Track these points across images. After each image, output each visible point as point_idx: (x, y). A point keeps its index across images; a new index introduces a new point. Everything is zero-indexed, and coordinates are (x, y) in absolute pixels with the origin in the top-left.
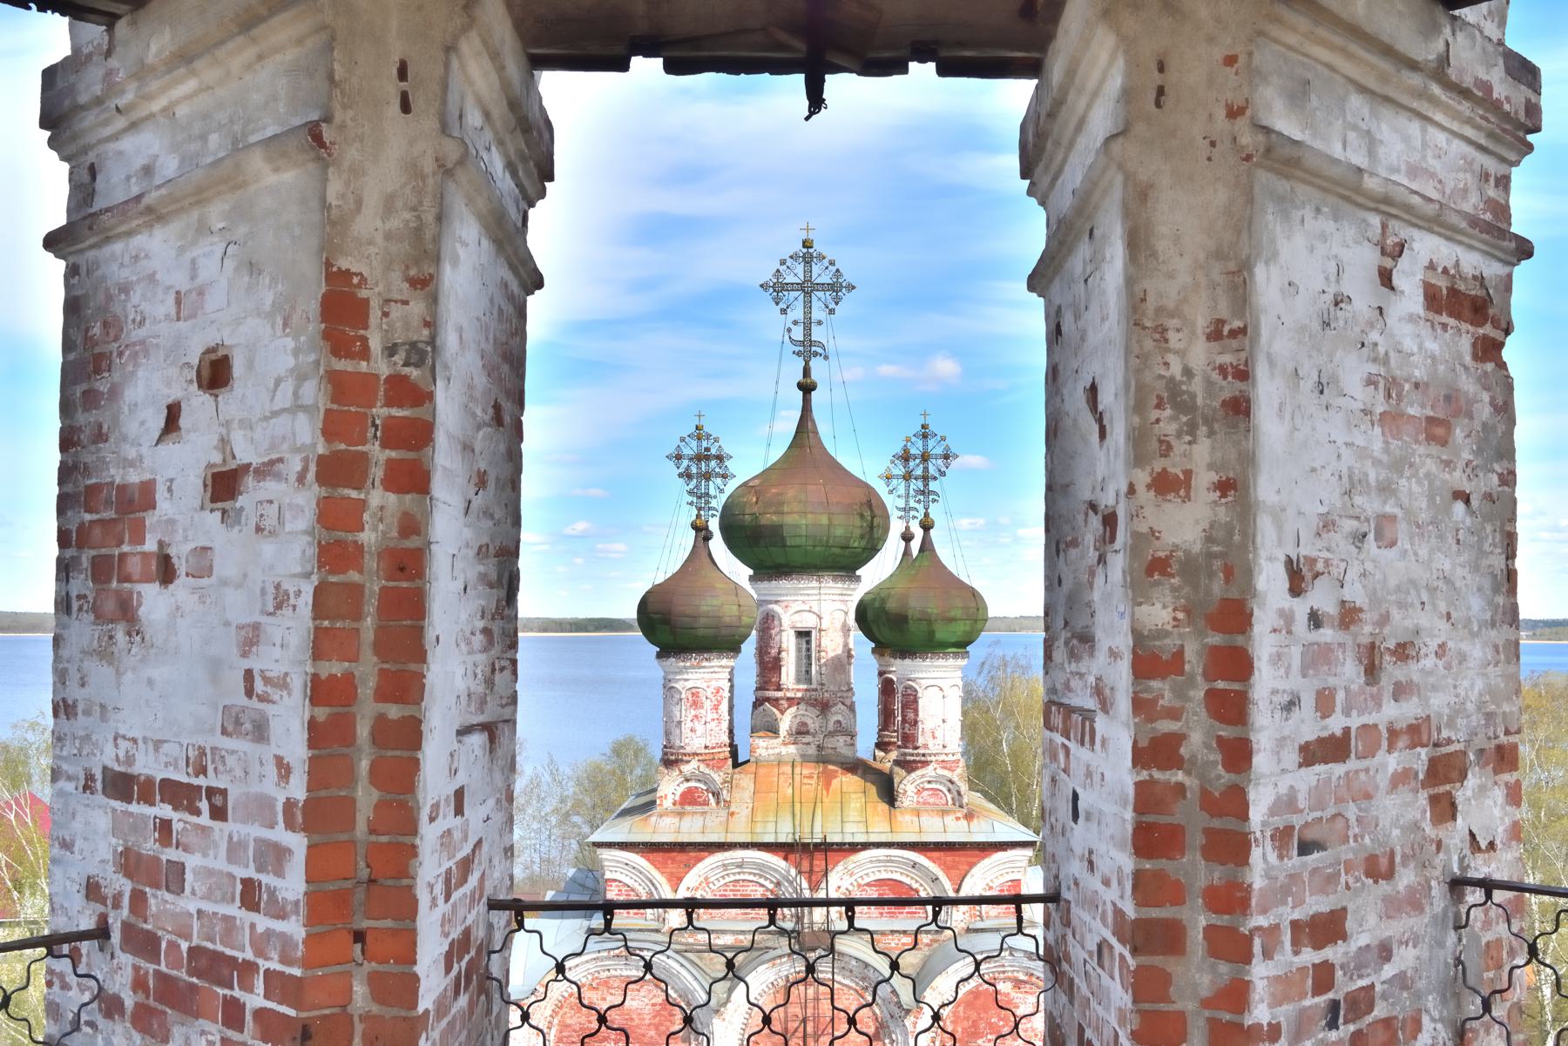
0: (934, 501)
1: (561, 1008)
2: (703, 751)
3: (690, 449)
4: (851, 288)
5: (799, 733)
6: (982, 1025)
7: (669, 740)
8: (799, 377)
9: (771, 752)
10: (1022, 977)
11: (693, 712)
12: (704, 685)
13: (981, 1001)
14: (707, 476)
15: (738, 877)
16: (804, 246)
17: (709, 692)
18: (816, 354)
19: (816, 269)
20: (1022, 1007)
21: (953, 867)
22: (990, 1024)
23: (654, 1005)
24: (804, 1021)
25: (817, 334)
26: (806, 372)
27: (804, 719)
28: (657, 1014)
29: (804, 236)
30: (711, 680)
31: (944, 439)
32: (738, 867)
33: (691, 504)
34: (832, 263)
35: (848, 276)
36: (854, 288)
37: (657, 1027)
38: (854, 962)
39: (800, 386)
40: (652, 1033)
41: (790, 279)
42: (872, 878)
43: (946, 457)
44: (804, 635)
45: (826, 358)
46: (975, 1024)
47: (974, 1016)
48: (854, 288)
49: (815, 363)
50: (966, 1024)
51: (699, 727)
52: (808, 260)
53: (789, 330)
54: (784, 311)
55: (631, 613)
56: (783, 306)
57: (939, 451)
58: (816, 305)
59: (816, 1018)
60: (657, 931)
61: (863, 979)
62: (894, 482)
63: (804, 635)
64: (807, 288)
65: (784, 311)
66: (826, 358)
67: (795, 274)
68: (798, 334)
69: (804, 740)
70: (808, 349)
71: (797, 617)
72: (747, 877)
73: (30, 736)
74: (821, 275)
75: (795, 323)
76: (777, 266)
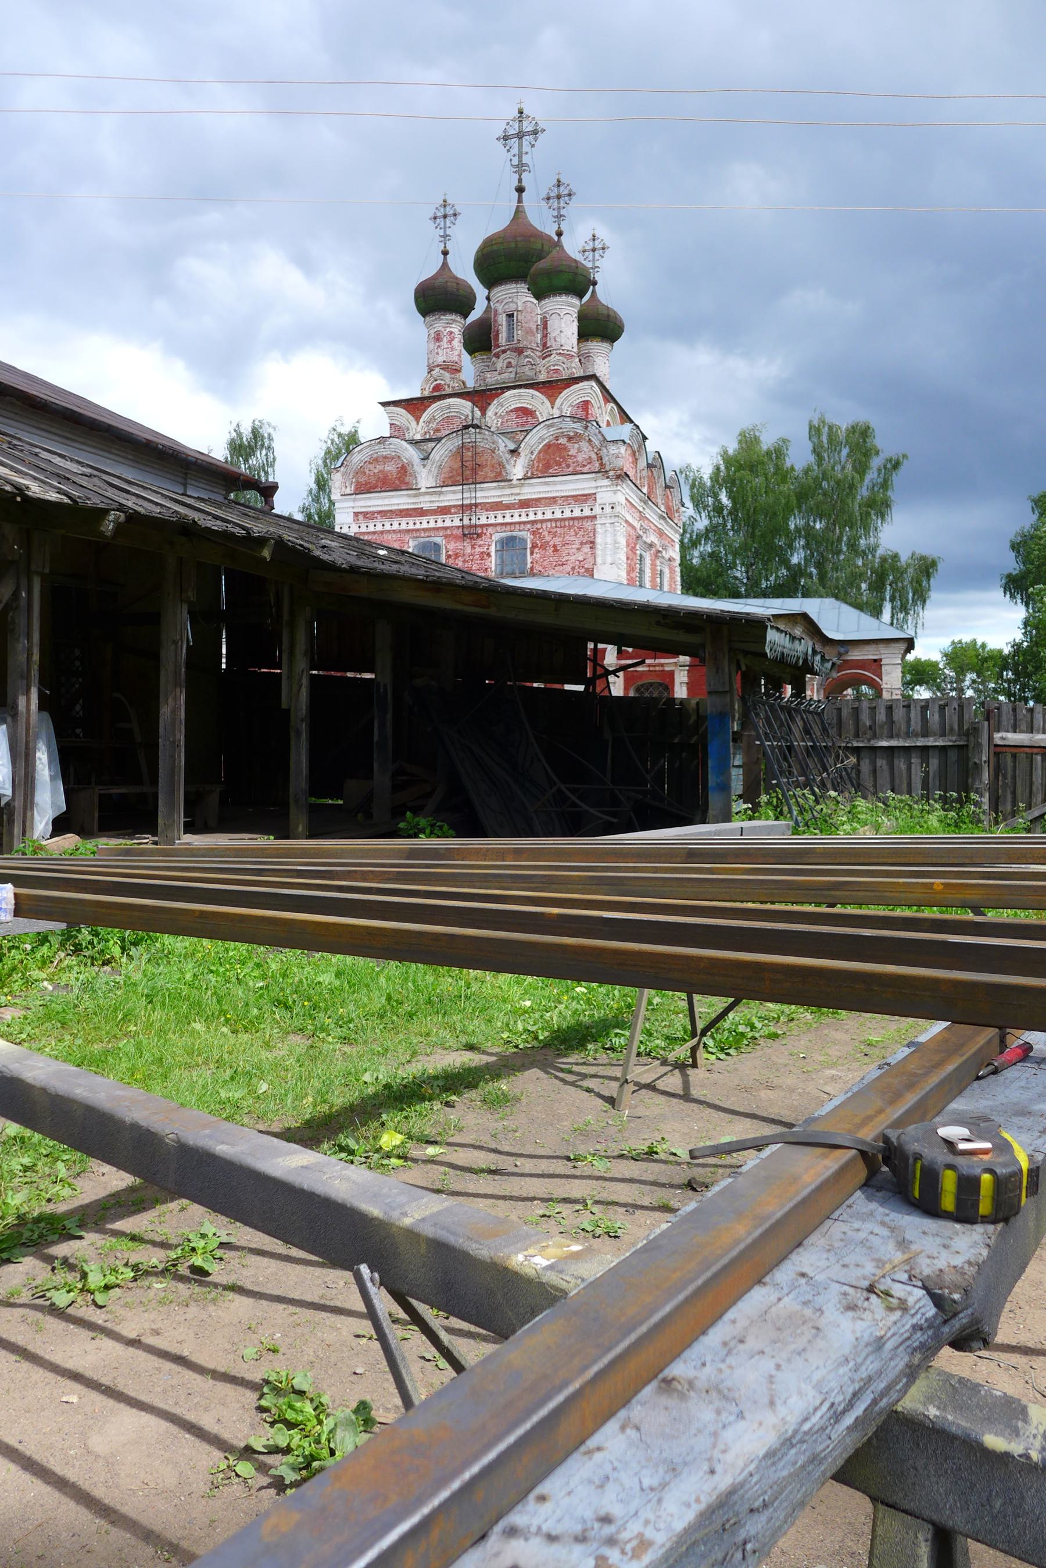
6: (552, 462)
8: (516, 183)
10: (572, 434)
12: (443, 330)
13: (552, 448)
18: (525, 170)
19: (525, 123)
21: (551, 396)
25: (526, 159)
26: (520, 180)
28: (399, 472)
29: (519, 106)
31: (568, 185)
32: (449, 408)
34: (533, 119)
37: (399, 479)
41: (511, 132)
42: (513, 407)
49: (524, 175)
50: (544, 462)
53: (511, 160)
54: (508, 151)
56: (507, 148)
57: (566, 192)
62: (587, 253)
63: (510, 316)
64: (520, 135)
65: (508, 151)
68: (515, 161)
69: (511, 369)
71: (506, 307)
72: (453, 414)
74: (527, 127)
75: (514, 155)
76: (505, 126)
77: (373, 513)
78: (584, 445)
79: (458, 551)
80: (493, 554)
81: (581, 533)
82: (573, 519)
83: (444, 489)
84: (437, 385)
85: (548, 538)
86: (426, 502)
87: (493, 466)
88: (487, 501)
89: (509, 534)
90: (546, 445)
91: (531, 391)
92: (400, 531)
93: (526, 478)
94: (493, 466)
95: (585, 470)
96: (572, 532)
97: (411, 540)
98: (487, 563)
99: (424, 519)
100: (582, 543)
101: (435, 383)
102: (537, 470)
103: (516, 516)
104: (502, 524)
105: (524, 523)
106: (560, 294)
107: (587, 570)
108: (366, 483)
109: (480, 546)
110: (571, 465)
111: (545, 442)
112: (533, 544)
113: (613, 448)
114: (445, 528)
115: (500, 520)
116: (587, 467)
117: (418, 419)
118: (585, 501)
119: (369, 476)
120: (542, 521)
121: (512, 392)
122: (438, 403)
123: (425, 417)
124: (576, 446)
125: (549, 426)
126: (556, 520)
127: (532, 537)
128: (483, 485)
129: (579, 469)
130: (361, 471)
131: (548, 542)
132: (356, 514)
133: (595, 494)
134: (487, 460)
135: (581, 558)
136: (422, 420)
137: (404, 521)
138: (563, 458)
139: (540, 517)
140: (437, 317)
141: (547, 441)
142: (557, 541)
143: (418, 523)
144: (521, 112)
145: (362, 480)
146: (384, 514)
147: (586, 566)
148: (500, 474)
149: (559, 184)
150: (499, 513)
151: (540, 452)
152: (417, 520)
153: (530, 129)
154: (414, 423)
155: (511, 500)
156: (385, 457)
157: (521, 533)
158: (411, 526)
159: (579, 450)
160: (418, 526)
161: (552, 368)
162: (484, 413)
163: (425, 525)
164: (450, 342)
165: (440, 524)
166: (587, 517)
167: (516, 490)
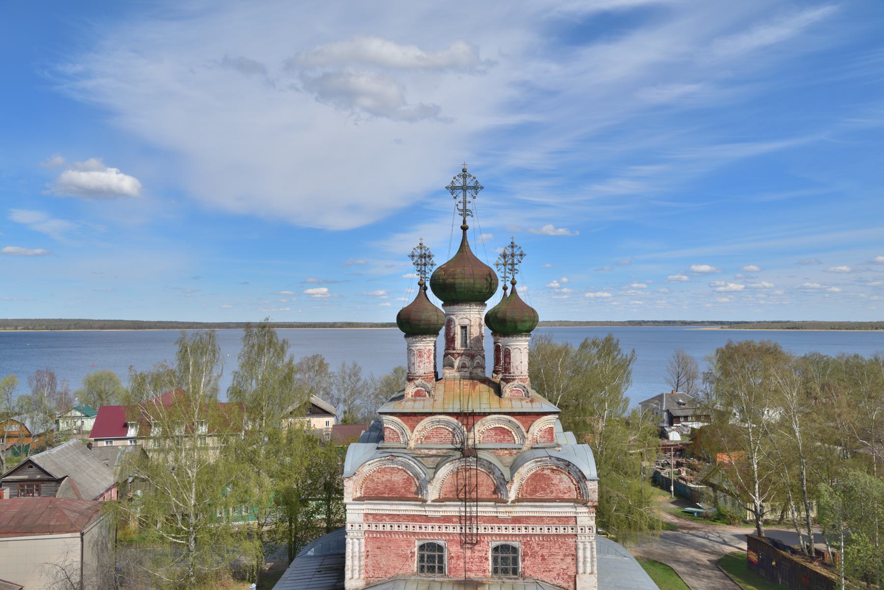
0: (516, 273)
1: (366, 480)
2: (423, 375)
3: (418, 252)
4: (482, 188)
5: (462, 367)
7: (409, 371)
8: (462, 224)
9: (451, 375)
10: (555, 468)
11: (419, 359)
12: (423, 348)
13: (538, 476)
14: (425, 265)
15: (438, 426)
16: (463, 171)
18: (468, 215)
19: (468, 180)
20: (555, 480)
21: (526, 422)
23: (404, 479)
24: (465, 486)
25: (468, 206)
26: (464, 222)
27: (464, 362)
30: (426, 346)
31: (520, 248)
33: (418, 275)
34: (474, 178)
35: (481, 183)
36: (483, 188)
37: (405, 488)
38: (485, 462)
39: (462, 228)
40: (403, 490)
41: (457, 184)
42: (492, 426)
43: (521, 255)
44: (464, 328)
45: (472, 216)
47: (535, 484)
48: (483, 188)
49: (467, 218)
50: (532, 487)
51: (422, 366)
52: (465, 177)
53: (457, 205)
54: (455, 198)
55: (395, 321)
56: (454, 195)
57: (518, 253)
58: (468, 194)
59: (470, 485)
60: (405, 448)
61: (489, 469)
62: (500, 266)
63: (464, 328)
64: (464, 188)
65: (455, 198)
66: (472, 216)
67: (459, 183)
68: (461, 206)
69: (465, 370)
70: (465, 212)
71: (461, 320)
72: (441, 426)
73: (161, 370)
74: (470, 182)
75: (460, 202)
77: (383, 515)
79: (460, 554)
80: (490, 558)
81: (565, 547)
84: (418, 390)
85: (537, 549)
86: (431, 512)
87: (488, 486)
88: (485, 515)
89: (503, 543)
90: (533, 474)
92: (407, 533)
93: (518, 500)
96: (557, 546)
98: (486, 566)
99: (430, 525)
100: (565, 555)
104: (497, 535)
105: (516, 535)
106: (522, 336)
107: (570, 577)
109: (479, 551)
110: (555, 491)
111: (532, 472)
112: (524, 552)
114: (449, 534)
116: (567, 495)
119: (377, 483)
120: (531, 535)
123: (419, 427)
124: (558, 477)
125: (537, 462)
126: (543, 535)
127: (523, 547)
129: (560, 495)
131: (537, 553)
134: (483, 481)
135: (565, 567)
136: (415, 430)
138: (548, 485)
141: (534, 471)
142: (545, 552)
143: (423, 527)
144: (464, 171)
145: (371, 485)
146: (393, 517)
147: (569, 574)
149: (512, 246)
151: (528, 479)
152: (423, 525)
153: (472, 184)
155: (506, 515)
157: (513, 543)
158: (417, 530)
159: (561, 481)
160: (423, 530)
161: (515, 389)
163: (430, 530)
165: (444, 530)
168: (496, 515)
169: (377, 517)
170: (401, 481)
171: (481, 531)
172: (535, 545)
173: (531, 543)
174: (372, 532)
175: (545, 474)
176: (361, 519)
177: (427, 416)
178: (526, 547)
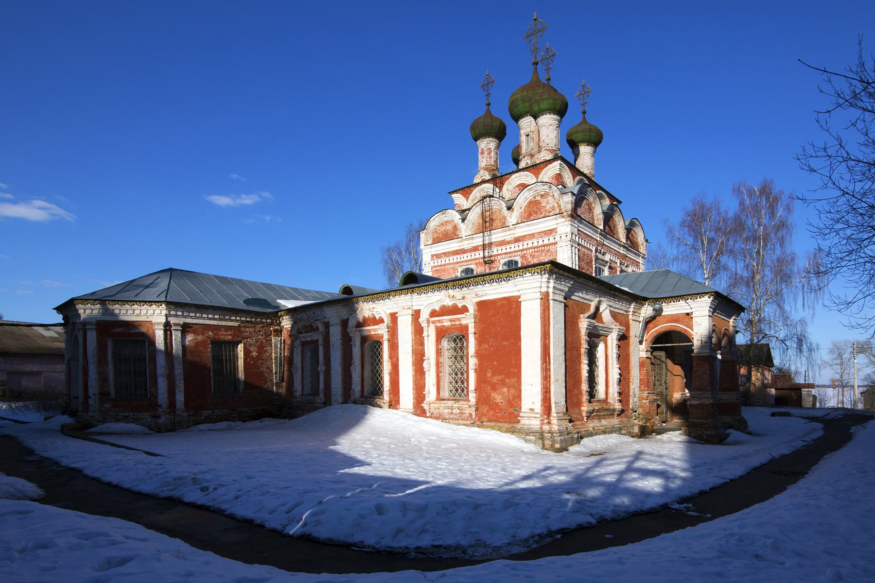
6: (532, 212)
10: (543, 193)
13: (532, 204)
17: (486, 149)
22: (534, 211)
28: (453, 229)
42: (517, 184)
46: (530, 213)
50: (528, 213)
77: (440, 254)
78: (550, 199)
81: (549, 254)
82: (544, 246)
83: (474, 236)
86: (466, 245)
89: (509, 259)
91: (525, 173)
94: (501, 219)
95: (551, 214)
96: (544, 255)
97: (459, 268)
101: (482, 178)
102: (524, 218)
103: (513, 247)
104: (505, 254)
105: (517, 251)
108: (438, 238)
109: (494, 268)
111: (528, 200)
113: (566, 198)
114: (476, 259)
115: (504, 251)
117: (467, 199)
118: (551, 234)
120: (527, 249)
121: (516, 175)
122: (478, 188)
123: (471, 197)
124: (546, 200)
127: (521, 259)
128: (494, 231)
129: (547, 214)
130: (435, 231)
132: (433, 256)
133: (556, 228)
134: (497, 216)
136: (469, 199)
137: (455, 257)
138: (539, 208)
139: (525, 246)
140: (481, 140)
141: (529, 199)
148: (504, 223)
150: (504, 247)
151: (525, 207)
152: (462, 256)
154: (466, 201)
156: (447, 222)
159: (548, 203)
162: (501, 188)
163: (466, 259)
164: (489, 154)
165: (473, 257)
166: (552, 244)
167: (512, 232)
168: (503, 239)
169: (438, 256)
170: (451, 228)
171: (495, 253)
172: (529, 256)
173: (526, 255)
174: (436, 267)
175: (537, 200)
176: (429, 258)
177: (475, 188)
178: (523, 259)
